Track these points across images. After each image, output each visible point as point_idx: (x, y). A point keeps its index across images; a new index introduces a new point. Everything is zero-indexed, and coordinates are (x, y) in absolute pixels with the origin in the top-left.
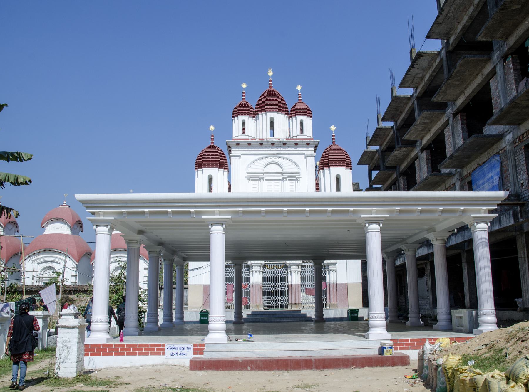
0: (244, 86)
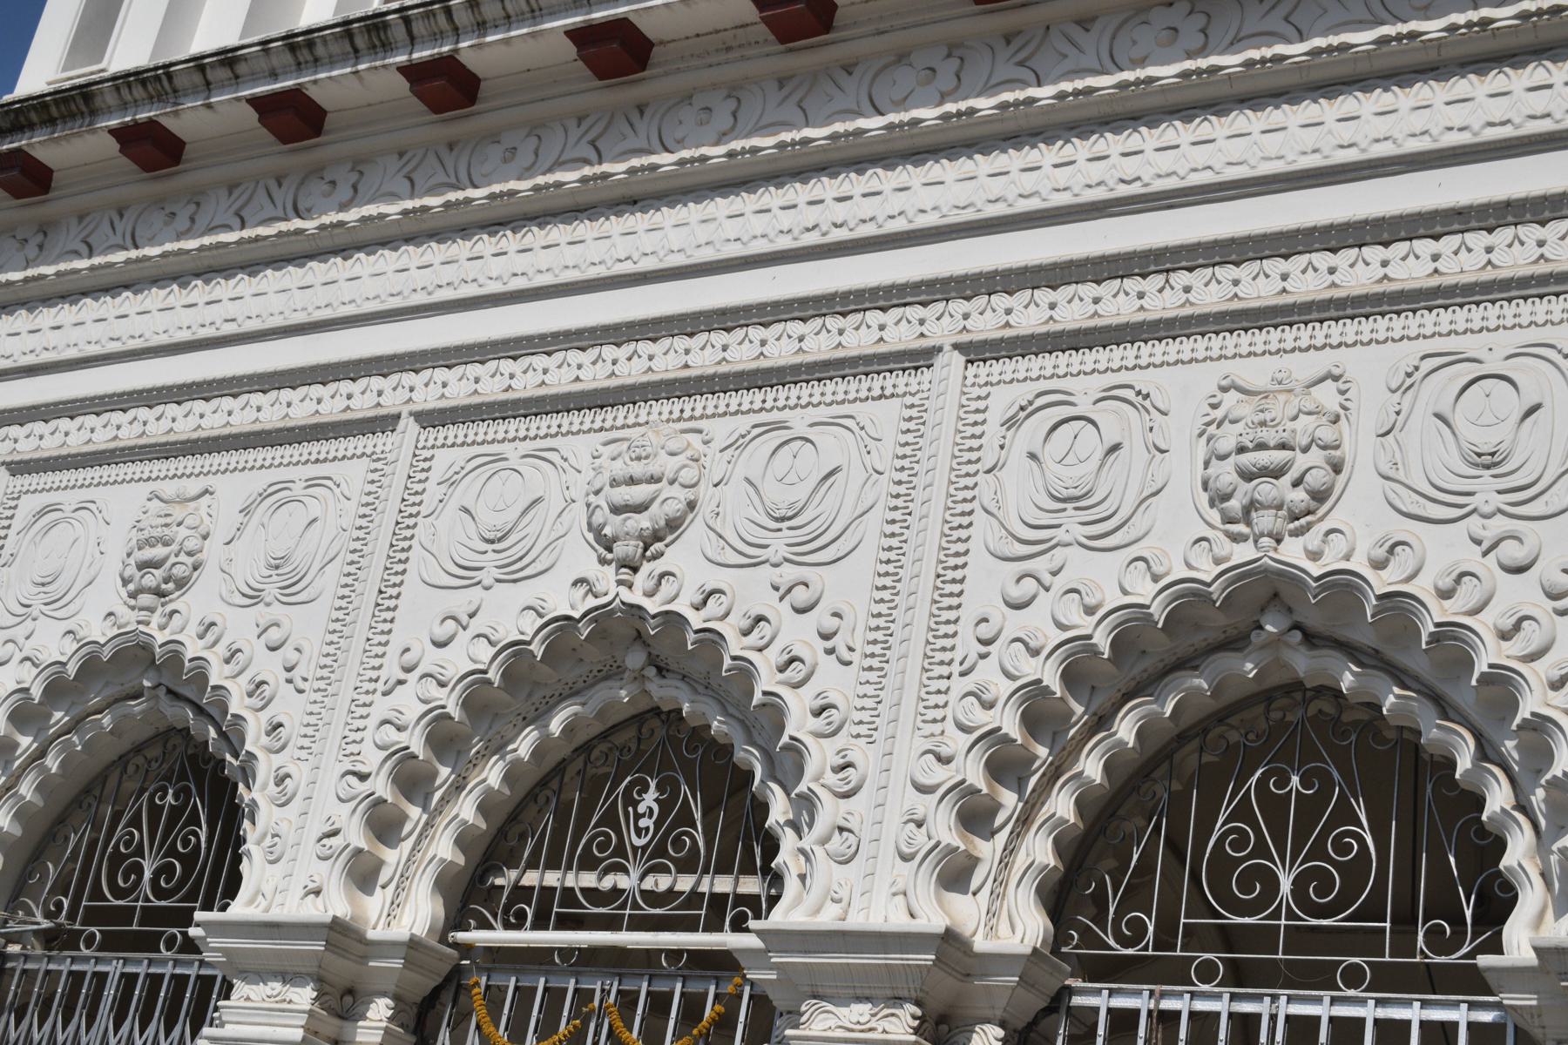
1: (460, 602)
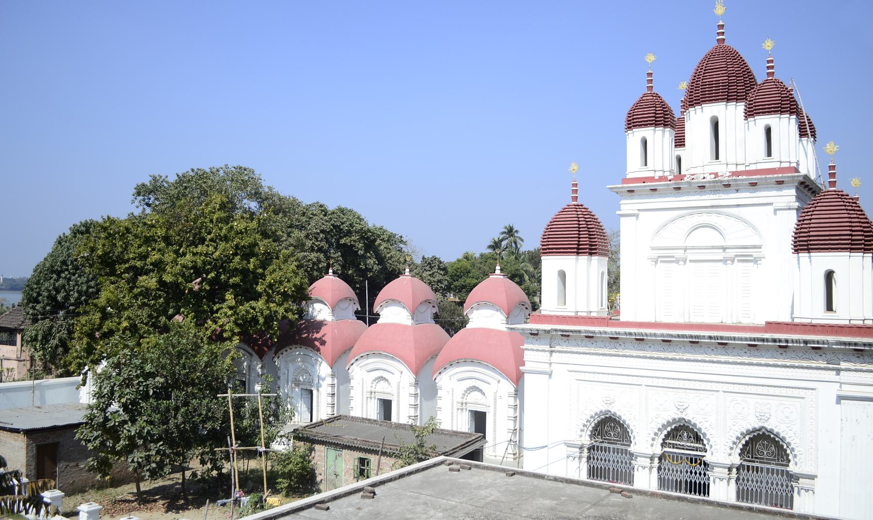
0: (650, 58)
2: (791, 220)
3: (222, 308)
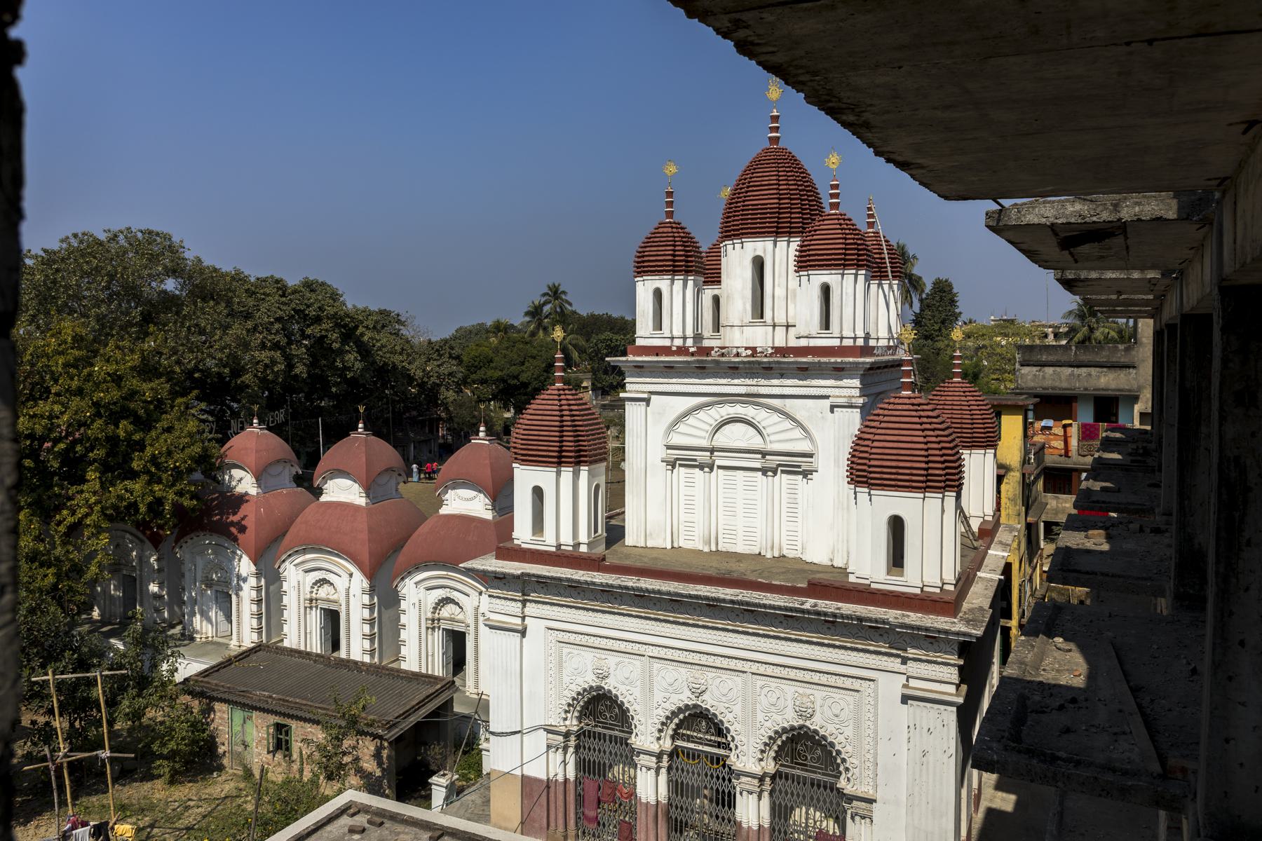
0: (672, 169)
1: (667, 695)
2: (852, 421)
3: (82, 492)
